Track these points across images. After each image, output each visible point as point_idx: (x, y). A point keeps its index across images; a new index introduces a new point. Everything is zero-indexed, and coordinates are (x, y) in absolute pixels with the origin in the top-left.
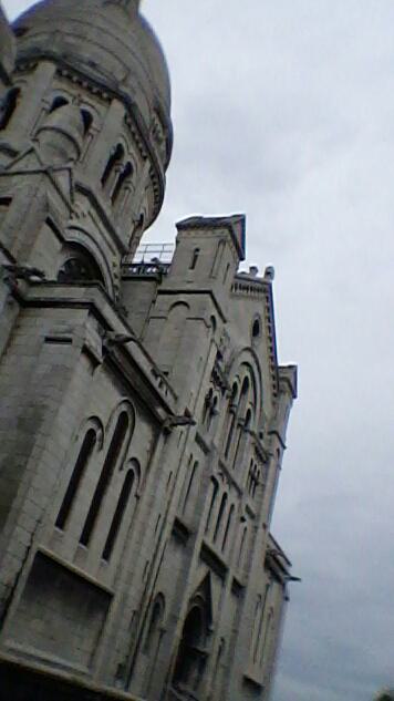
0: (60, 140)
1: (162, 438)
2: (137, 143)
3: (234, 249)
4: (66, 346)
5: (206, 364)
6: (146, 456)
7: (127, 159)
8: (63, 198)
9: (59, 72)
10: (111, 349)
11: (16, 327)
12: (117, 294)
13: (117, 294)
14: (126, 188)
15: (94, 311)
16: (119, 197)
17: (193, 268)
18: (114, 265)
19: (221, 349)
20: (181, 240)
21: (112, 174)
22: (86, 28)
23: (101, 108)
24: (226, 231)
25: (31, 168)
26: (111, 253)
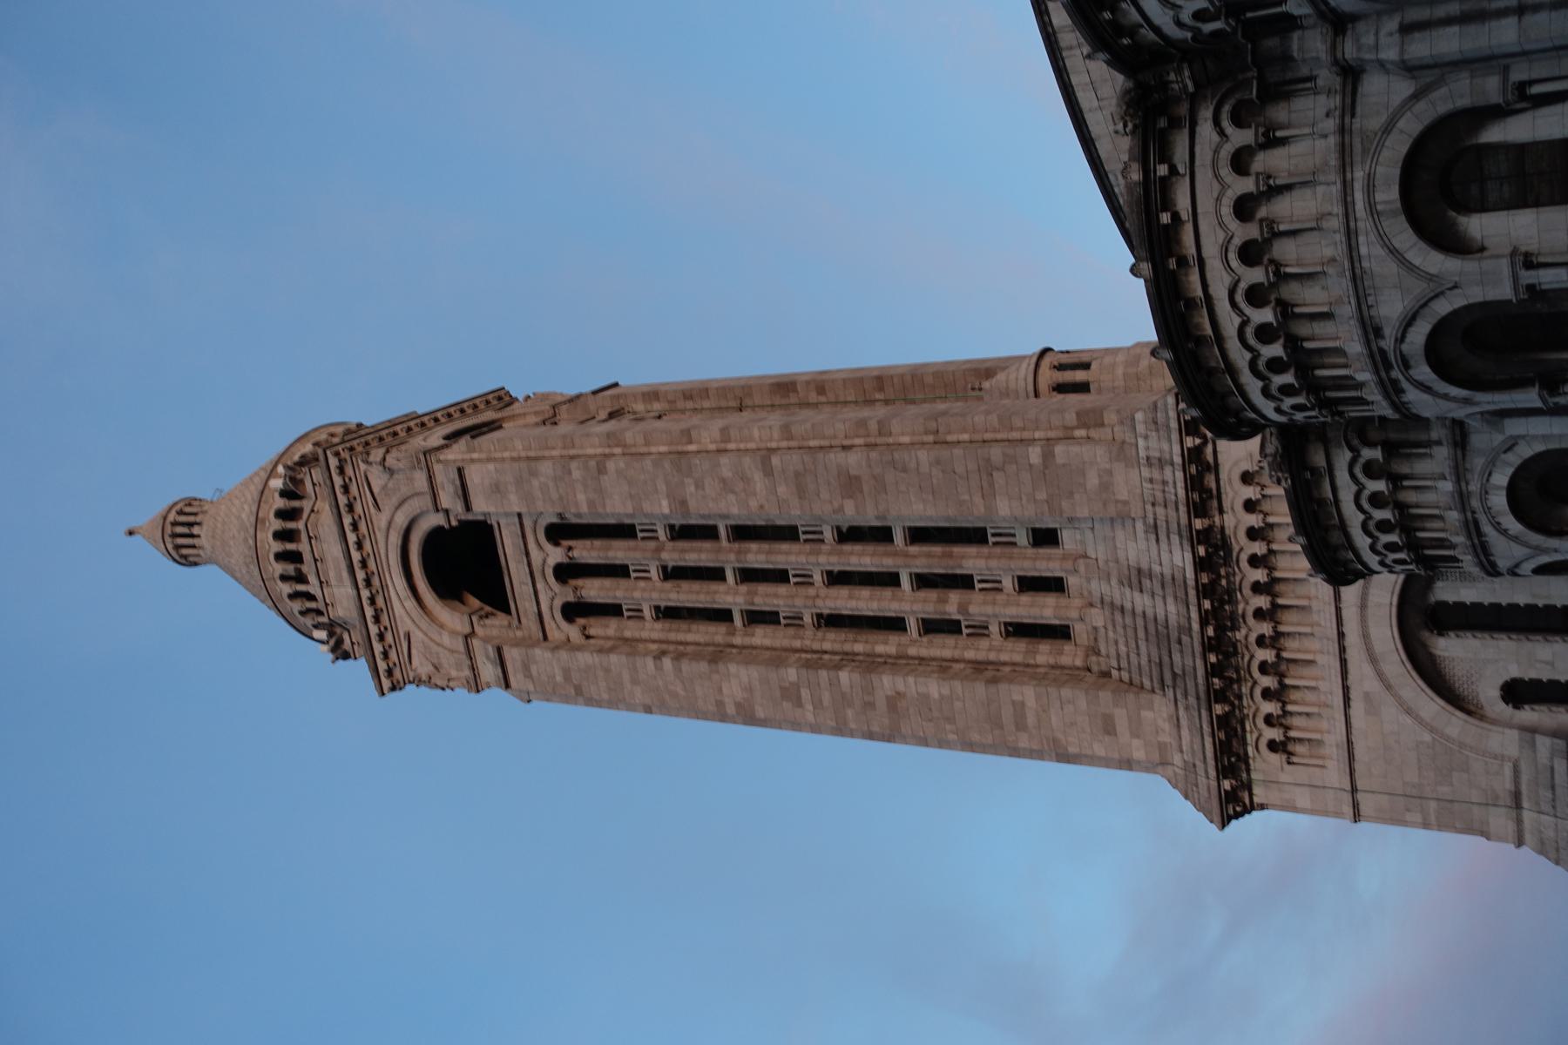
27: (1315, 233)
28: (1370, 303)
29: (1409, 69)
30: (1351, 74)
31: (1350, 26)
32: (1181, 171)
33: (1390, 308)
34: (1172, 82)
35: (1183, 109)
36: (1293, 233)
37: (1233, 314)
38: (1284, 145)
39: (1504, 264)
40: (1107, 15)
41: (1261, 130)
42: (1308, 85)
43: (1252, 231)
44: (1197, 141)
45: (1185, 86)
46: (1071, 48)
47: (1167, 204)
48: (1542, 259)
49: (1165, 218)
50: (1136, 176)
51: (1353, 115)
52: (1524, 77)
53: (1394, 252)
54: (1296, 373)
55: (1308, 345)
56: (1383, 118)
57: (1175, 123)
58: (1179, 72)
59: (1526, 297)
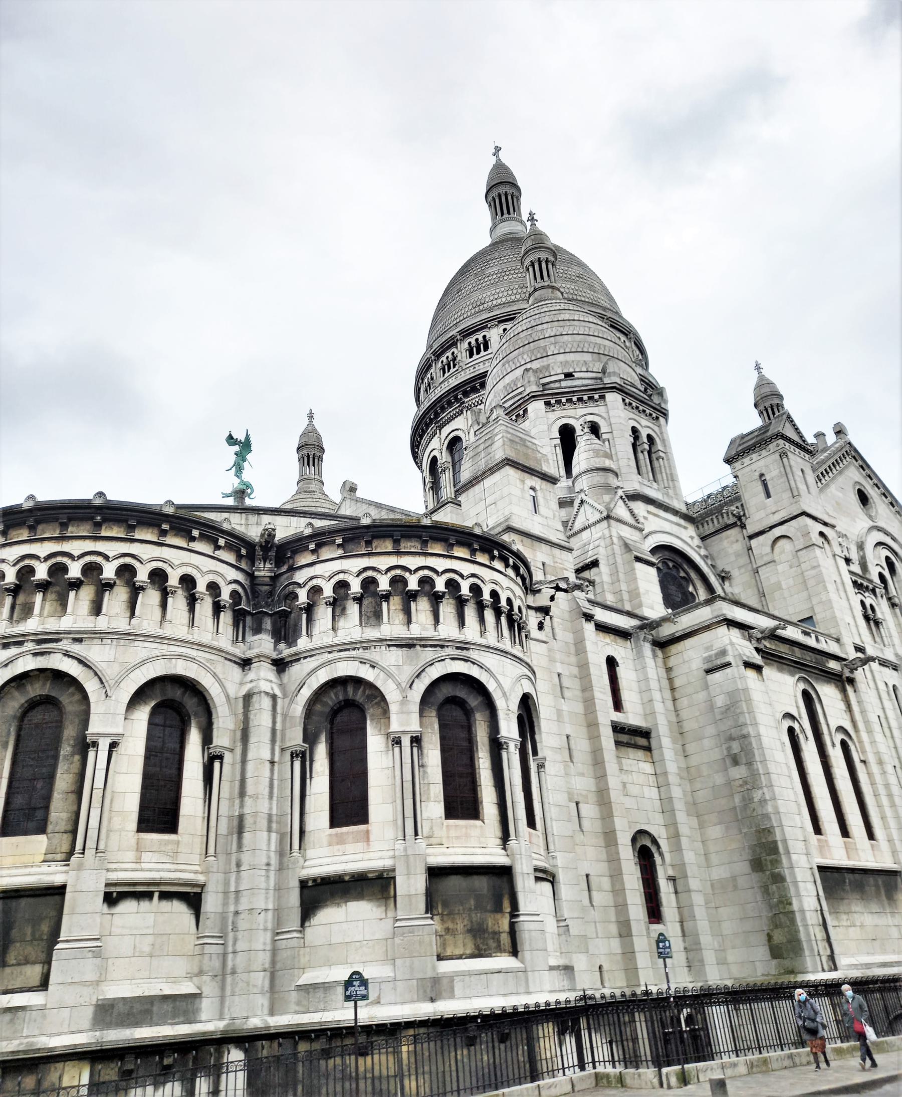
0: (598, 478)
1: (849, 689)
2: (644, 411)
3: (797, 450)
4: (728, 670)
5: (843, 584)
6: (847, 717)
7: (644, 433)
8: (631, 526)
9: (548, 404)
10: (761, 646)
11: (669, 670)
12: (710, 562)
13: (710, 562)
14: (657, 459)
15: (732, 623)
16: (657, 470)
17: (768, 495)
18: (692, 538)
19: (846, 553)
20: (739, 474)
21: (640, 455)
22: (542, 343)
23: (600, 410)
24: (781, 442)
25: (591, 521)
26: (683, 530)
27: (159, 619)
28: (104, 640)
29: (248, 698)
30: (245, 663)
31: (275, 668)
32: (216, 552)
33: (94, 652)
34: (264, 564)
35: (243, 566)
36: (164, 605)
37: (117, 553)
38: (214, 615)
39: (120, 731)
40: (339, 541)
41: (227, 605)
42: (240, 638)
43: (173, 581)
44: (229, 567)
45: (260, 571)
46: (247, 519)
47: (203, 537)
48: (114, 754)
49: (195, 533)
50: (226, 526)
51: (226, 659)
52: (225, 760)
53: (143, 663)
54: (47, 581)
55: (72, 594)
56: (221, 676)
57: (239, 557)
58: (270, 571)
59: (88, 741)
